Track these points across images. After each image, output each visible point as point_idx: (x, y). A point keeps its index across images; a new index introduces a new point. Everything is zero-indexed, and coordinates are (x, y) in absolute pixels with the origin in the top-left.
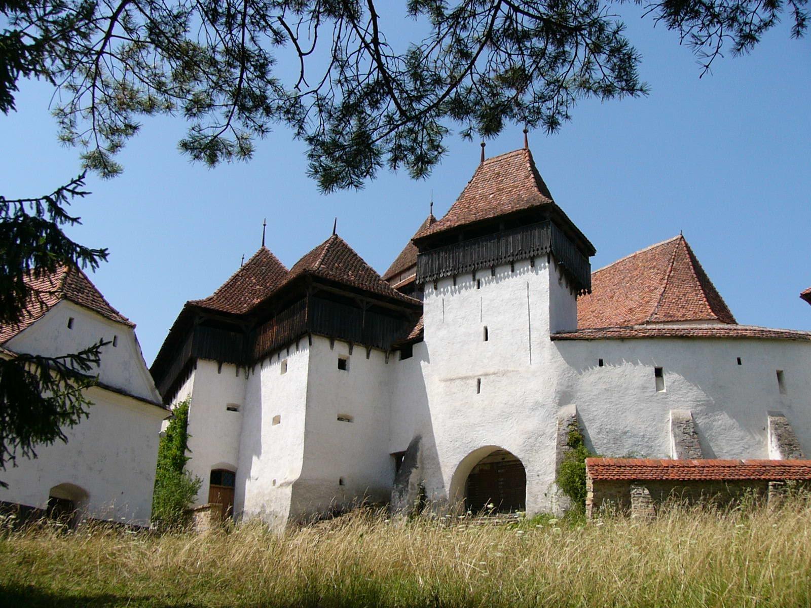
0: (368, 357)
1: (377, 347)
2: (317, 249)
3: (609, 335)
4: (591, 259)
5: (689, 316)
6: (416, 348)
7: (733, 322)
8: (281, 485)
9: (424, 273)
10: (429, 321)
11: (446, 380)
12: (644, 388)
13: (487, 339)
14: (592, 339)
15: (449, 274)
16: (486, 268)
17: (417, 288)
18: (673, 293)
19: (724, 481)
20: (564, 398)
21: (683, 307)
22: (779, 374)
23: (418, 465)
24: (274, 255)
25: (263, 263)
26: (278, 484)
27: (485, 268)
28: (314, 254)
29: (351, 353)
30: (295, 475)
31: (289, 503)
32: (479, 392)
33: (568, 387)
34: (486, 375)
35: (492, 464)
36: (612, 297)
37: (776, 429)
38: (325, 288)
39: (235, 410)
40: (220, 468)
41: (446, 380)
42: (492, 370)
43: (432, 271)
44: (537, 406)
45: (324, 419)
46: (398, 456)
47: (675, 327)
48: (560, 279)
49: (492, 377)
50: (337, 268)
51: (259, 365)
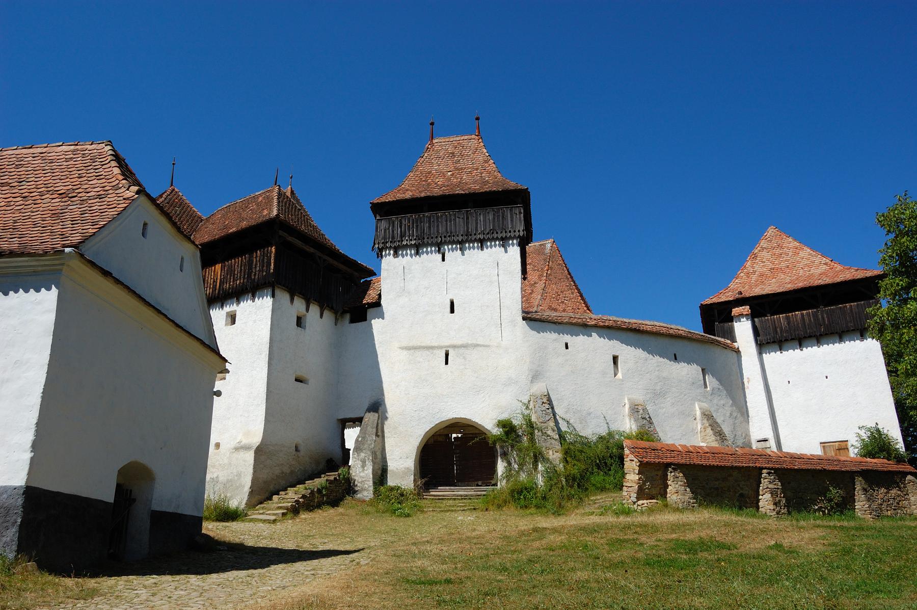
0: (321, 316)
1: (332, 309)
6: (370, 312)
9: (384, 238)
11: (408, 348)
13: (452, 311)
14: (560, 323)
18: (552, 289)
19: (732, 468)
20: (535, 377)
21: (563, 302)
29: (307, 310)
30: (256, 438)
32: (447, 363)
33: (539, 366)
34: (454, 347)
38: (290, 239)
41: (408, 348)
42: (460, 342)
43: (393, 238)
45: (285, 379)
49: (462, 350)
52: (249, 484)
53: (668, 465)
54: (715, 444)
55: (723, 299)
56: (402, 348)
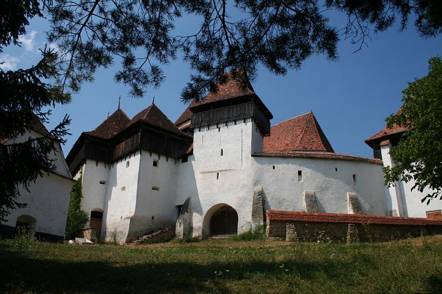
0: (167, 161)
1: (171, 157)
2: (144, 110)
3: (278, 155)
4: (271, 120)
5: (313, 149)
6: (189, 158)
7: (334, 152)
8: (125, 219)
10: (196, 145)
11: (202, 173)
12: (293, 180)
13: (222, 155)
15: (206, 124)
16: (223, 123)
17: (191, 130)
20: (256, 183)
21: (311, 144)
22: (354, 176)
23: (189, 211)
24: (124, 112)
25: (119, 115)
26: (123, 218)
27: (223, 123)
28: (143, 112)
30: (132, 214)
31: (129, 227)
32: (218, 179)
34: (221, 171)
35: (222, 212)
36: (279, 139)
37: (351, 201)
39: (103, 183)
40: (98, 210)
41: (202, 173)
42: (224, 169)
44: (244, 186)
45: (146, 189)
46: (179, 207)
47: (308, 153)
48: (256, 129)
49: (224, 172)
50: (154, 119)
51: (116, 163)
52: (127, 233)
53: (287, 221)
54: (350, 211)
55: (377, 137)
56: (200, 173)
